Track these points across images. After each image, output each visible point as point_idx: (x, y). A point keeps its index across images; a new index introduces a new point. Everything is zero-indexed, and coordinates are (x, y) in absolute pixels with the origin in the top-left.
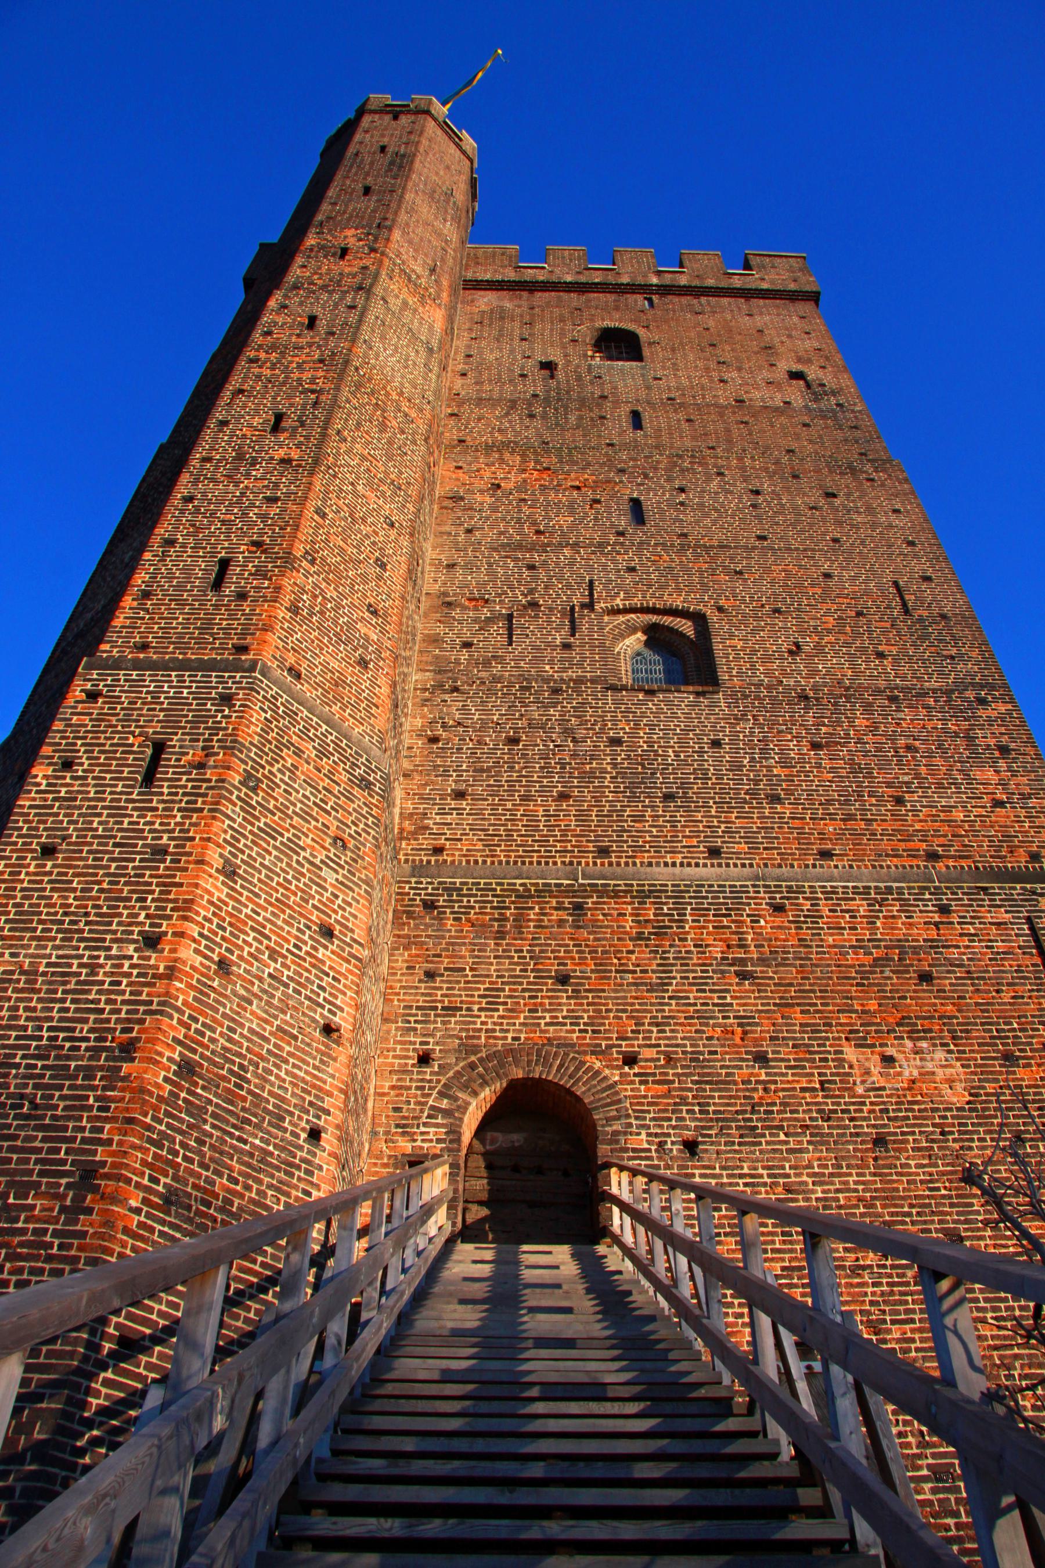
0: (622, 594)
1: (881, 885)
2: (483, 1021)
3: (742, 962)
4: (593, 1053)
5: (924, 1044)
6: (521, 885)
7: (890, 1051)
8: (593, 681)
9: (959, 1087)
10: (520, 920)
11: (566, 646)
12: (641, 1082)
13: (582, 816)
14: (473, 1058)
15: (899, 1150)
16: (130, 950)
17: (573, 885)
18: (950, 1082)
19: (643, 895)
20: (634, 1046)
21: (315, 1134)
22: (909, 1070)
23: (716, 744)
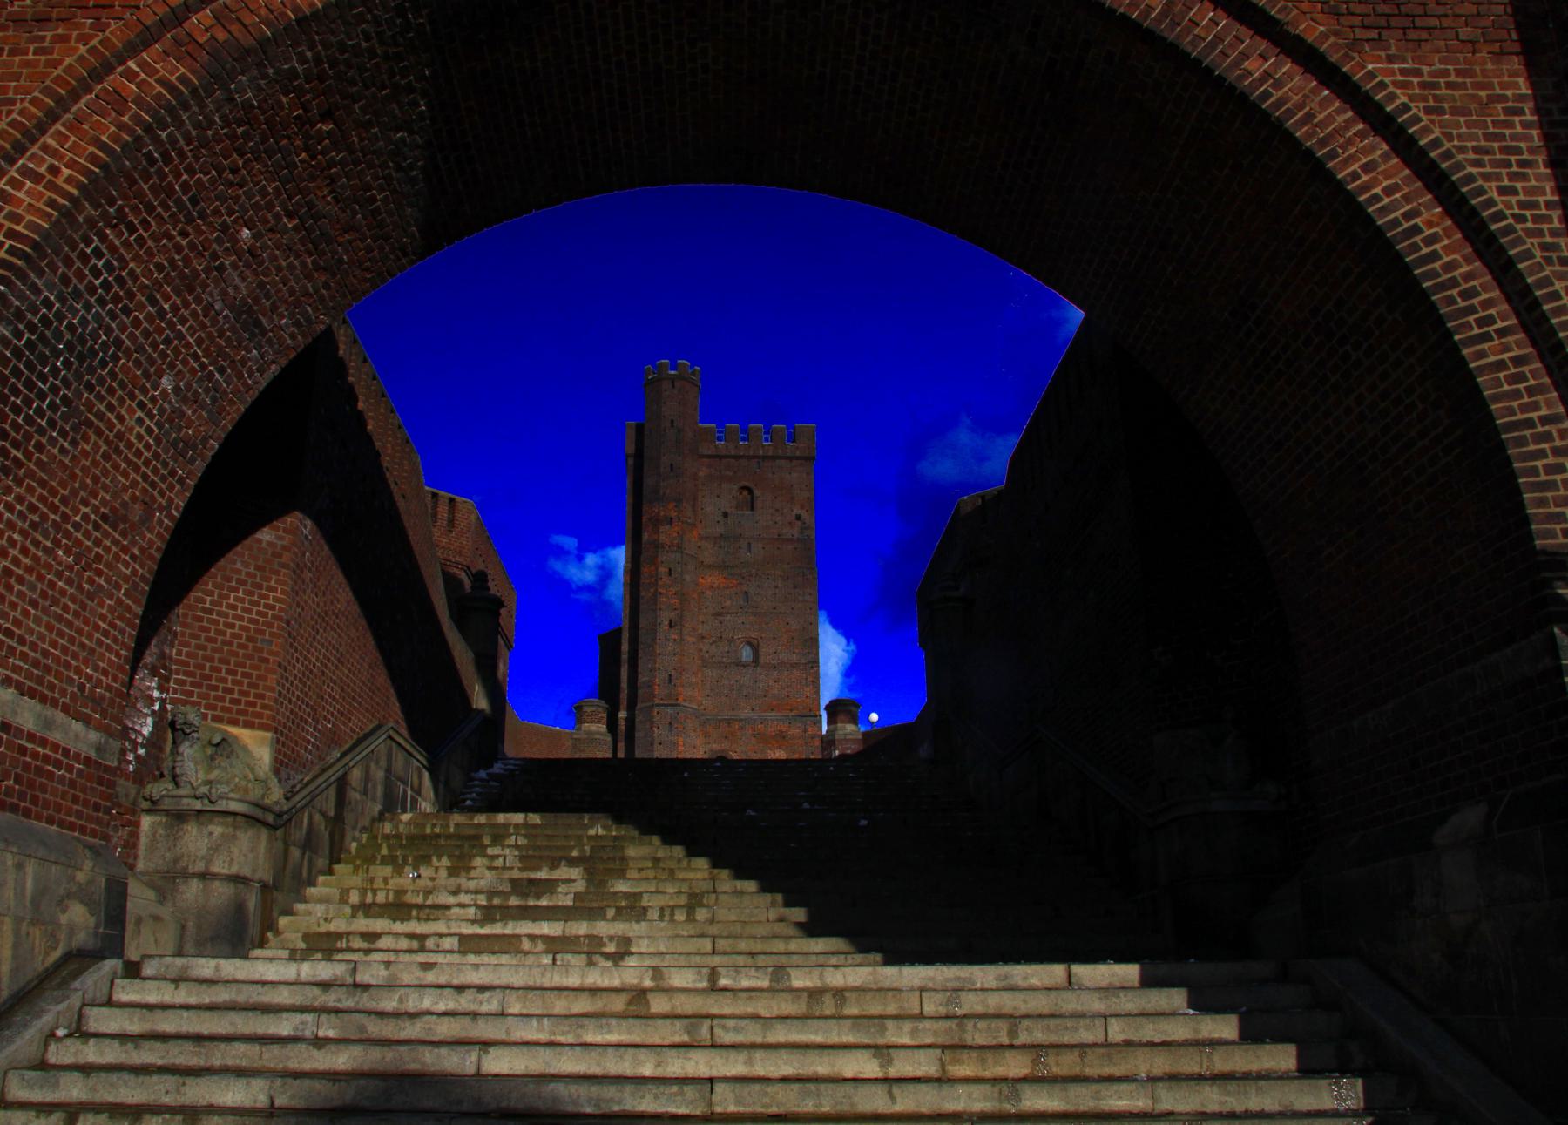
19: (741, 720)
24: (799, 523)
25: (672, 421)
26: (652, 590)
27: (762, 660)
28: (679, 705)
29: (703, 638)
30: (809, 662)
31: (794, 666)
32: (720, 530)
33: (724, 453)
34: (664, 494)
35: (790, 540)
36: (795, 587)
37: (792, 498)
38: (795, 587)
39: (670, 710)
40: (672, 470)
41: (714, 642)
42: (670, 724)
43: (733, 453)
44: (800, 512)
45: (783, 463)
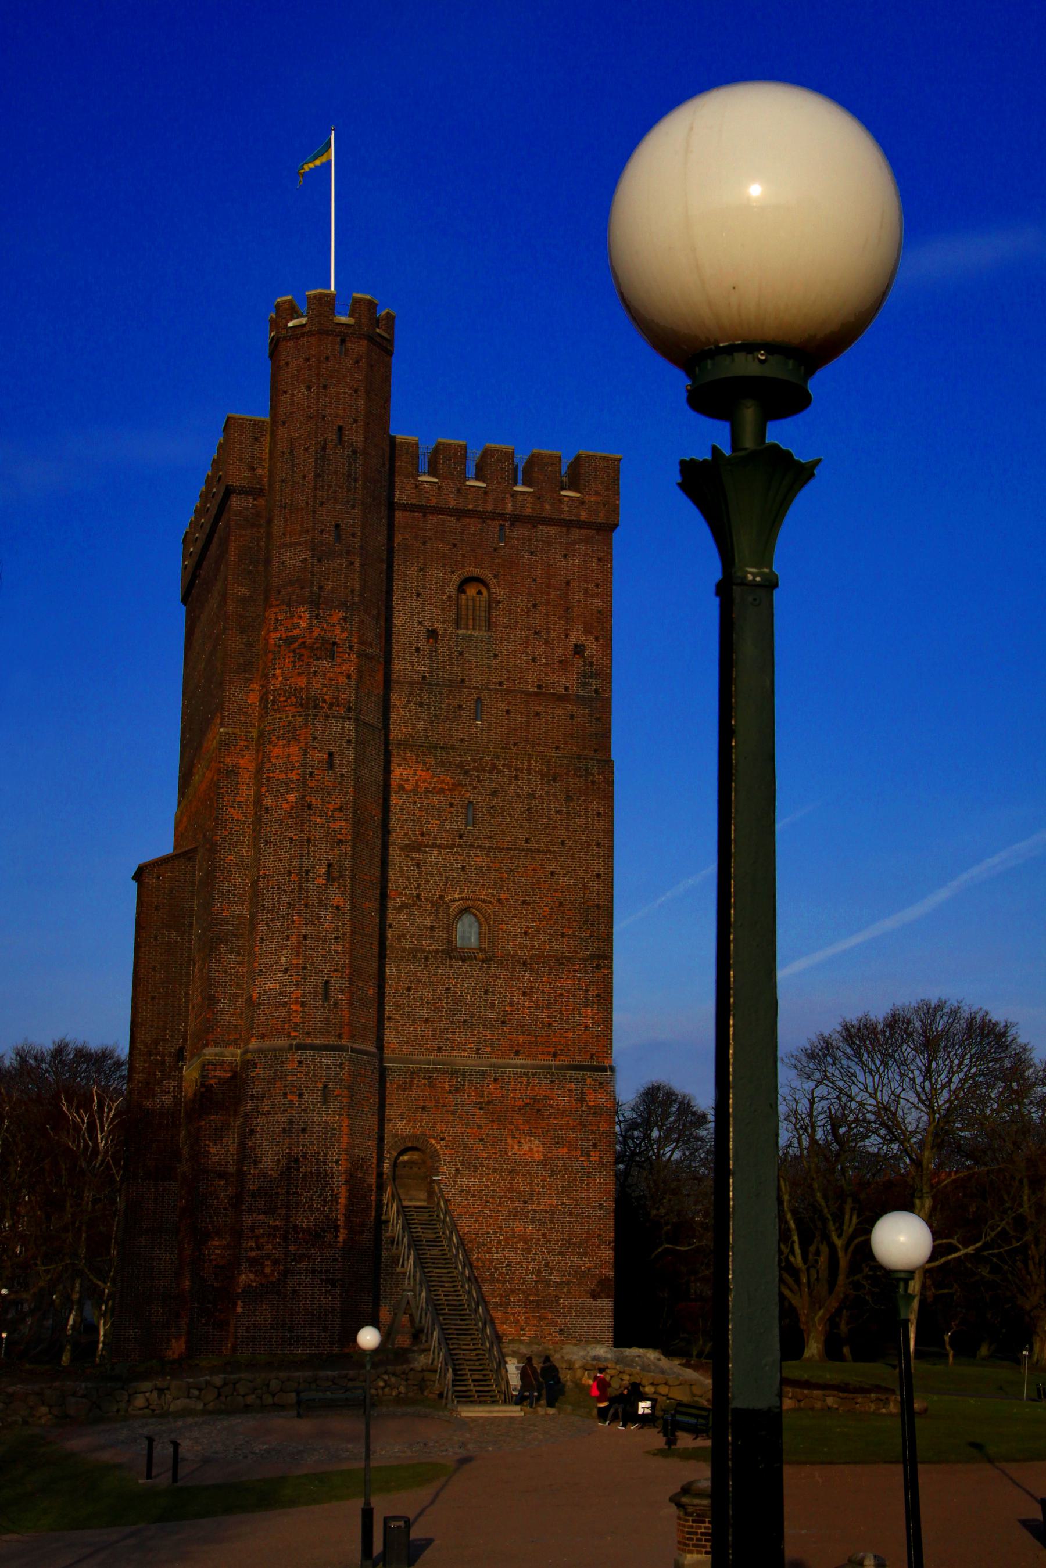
0: (458, 890)
1: (534, 1071)
3: (481, 1103)
4: (433, 1138)
5: (533, 1138)
6: (412, 1067)
7: (522, 1140)
8: (443, 951)
9: (540, 1154)
10: (411, 1082)
11: (432, 928)
12: (446, 1149)
13: (434, 1030)
14: (397, 1139)
15: (517, 1175)
16: (334, 1165)
17: (429, 1068)
18: (537, 1152)
23: (486, 992)
24: (578, 661)
25: (340, 429)
26: (292, 798)
30: (593, 957)
31: (561, 962)
32: (421, 667)
33: (434, 502)
34: (321, 588)
35: (563, 698)
38: (569, 798)
39: (324, 1059)
40: (338, 538)
41: (405, 906)
42: (325, 1087)
43: (452, 503)
44: (583, 638)
45: (553, 530)
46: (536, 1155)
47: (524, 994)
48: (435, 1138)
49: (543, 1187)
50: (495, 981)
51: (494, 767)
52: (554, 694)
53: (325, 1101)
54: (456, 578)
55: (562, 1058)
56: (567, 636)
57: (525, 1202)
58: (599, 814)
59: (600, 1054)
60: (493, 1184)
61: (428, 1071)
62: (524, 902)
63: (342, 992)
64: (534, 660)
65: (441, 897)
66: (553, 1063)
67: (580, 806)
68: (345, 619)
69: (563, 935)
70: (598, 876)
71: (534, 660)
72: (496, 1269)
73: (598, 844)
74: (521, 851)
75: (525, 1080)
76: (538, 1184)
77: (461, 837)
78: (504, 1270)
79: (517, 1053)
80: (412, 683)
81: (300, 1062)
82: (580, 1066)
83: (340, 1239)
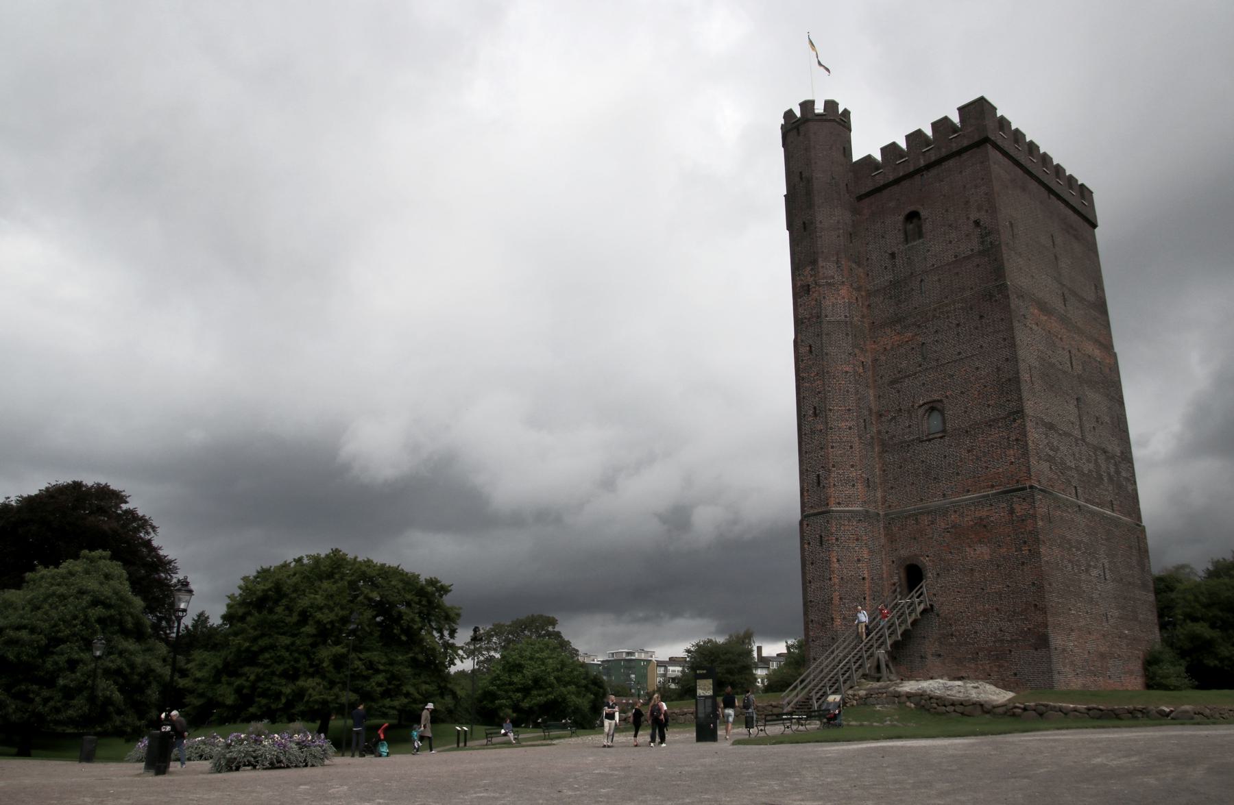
2: (902, 552)
3: (948, 528)
8: (917, 439)
11: (910, 426)
19: (928, 513)
20: (928, 553)
21: (865, 598)
22: (978, 552)
23: (945, 457)
25: (801, 173)
27: (949, 426)
28: (833, 511)
29: (881, 415)
31: (991, 423)
33: (882, 183)
36: (981, 317)
37: (967, 202)
38: (981, 317)
41: (894, 418)
42: (821, 536)
43: (891, 178)
45: (951, 162)
46: (985, 556)
47: (969, 451)
48: (922, 556)
49: (992, 577)
50: (949, 448)
51: (934, 316)
52: (964, 257)
53: (821, 544)
54: (901, 218)
55: (997, 488)
56: (968, 218)
57: (983, 589)
58: (1002, 319)
59: (1022, 479)
60: (960, 579)
61: (915, 515)
62: (962, 393)
63: (826, 479)
64: (950, 242)
65: (913, 406)
66: (989, 493)
67: (989, 319)
68: (812, 270)
69: (989, 406)
70: (1007, 359)
71: (950, 242)
72: (968, 636)
73: (1005, 339)
74: (955, 361)
75: (973, 508)
76: (989, 575)
77: (920, 366)
78: (973, 636)
79: (968, 491)
80: (884, 289)
81: (808, 525)
82: (1010, 490)
83: (834, 625)
